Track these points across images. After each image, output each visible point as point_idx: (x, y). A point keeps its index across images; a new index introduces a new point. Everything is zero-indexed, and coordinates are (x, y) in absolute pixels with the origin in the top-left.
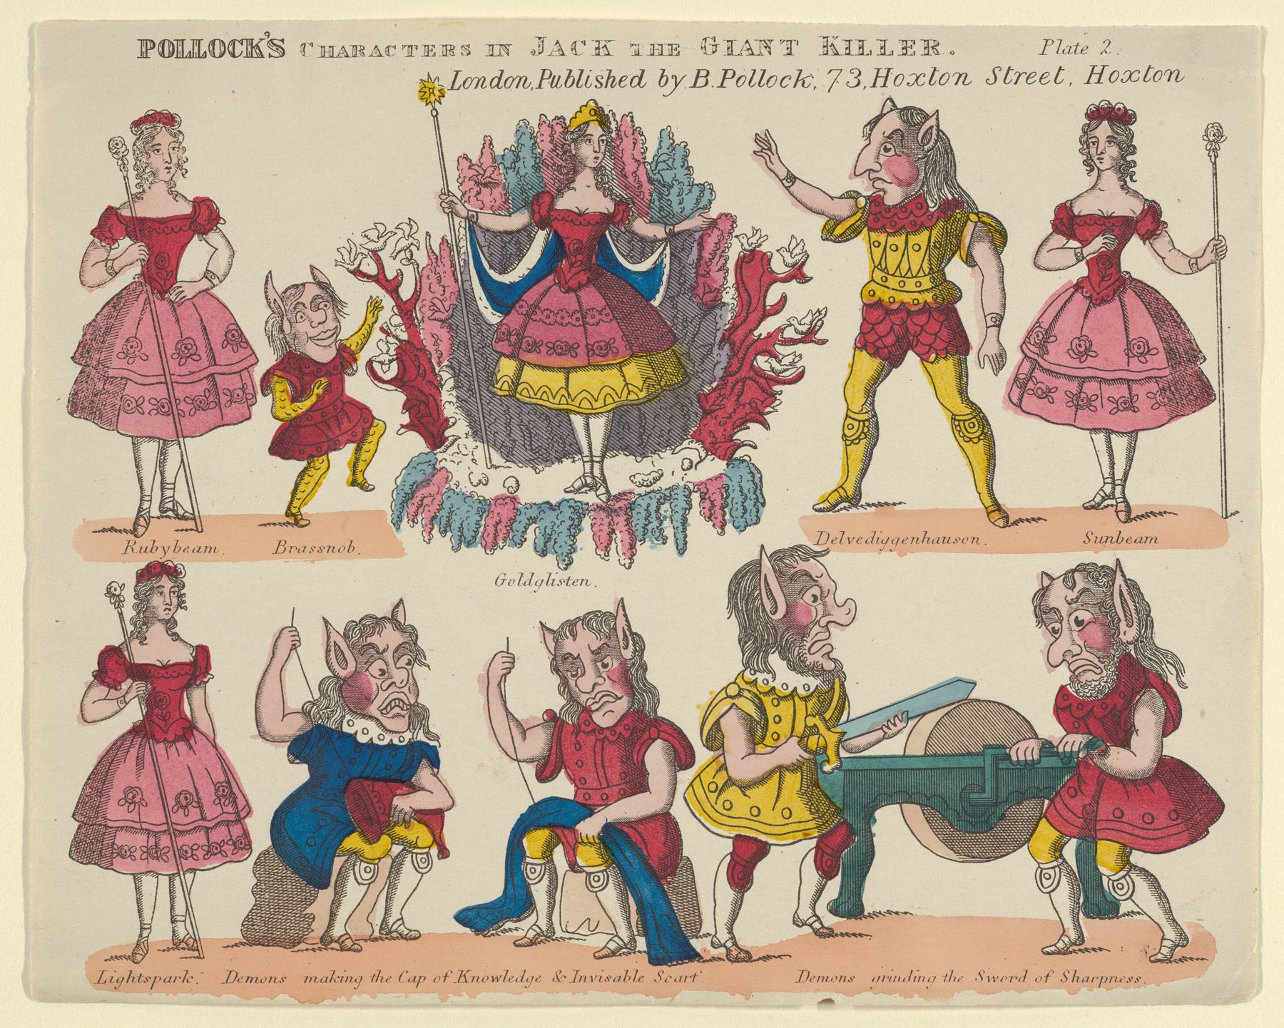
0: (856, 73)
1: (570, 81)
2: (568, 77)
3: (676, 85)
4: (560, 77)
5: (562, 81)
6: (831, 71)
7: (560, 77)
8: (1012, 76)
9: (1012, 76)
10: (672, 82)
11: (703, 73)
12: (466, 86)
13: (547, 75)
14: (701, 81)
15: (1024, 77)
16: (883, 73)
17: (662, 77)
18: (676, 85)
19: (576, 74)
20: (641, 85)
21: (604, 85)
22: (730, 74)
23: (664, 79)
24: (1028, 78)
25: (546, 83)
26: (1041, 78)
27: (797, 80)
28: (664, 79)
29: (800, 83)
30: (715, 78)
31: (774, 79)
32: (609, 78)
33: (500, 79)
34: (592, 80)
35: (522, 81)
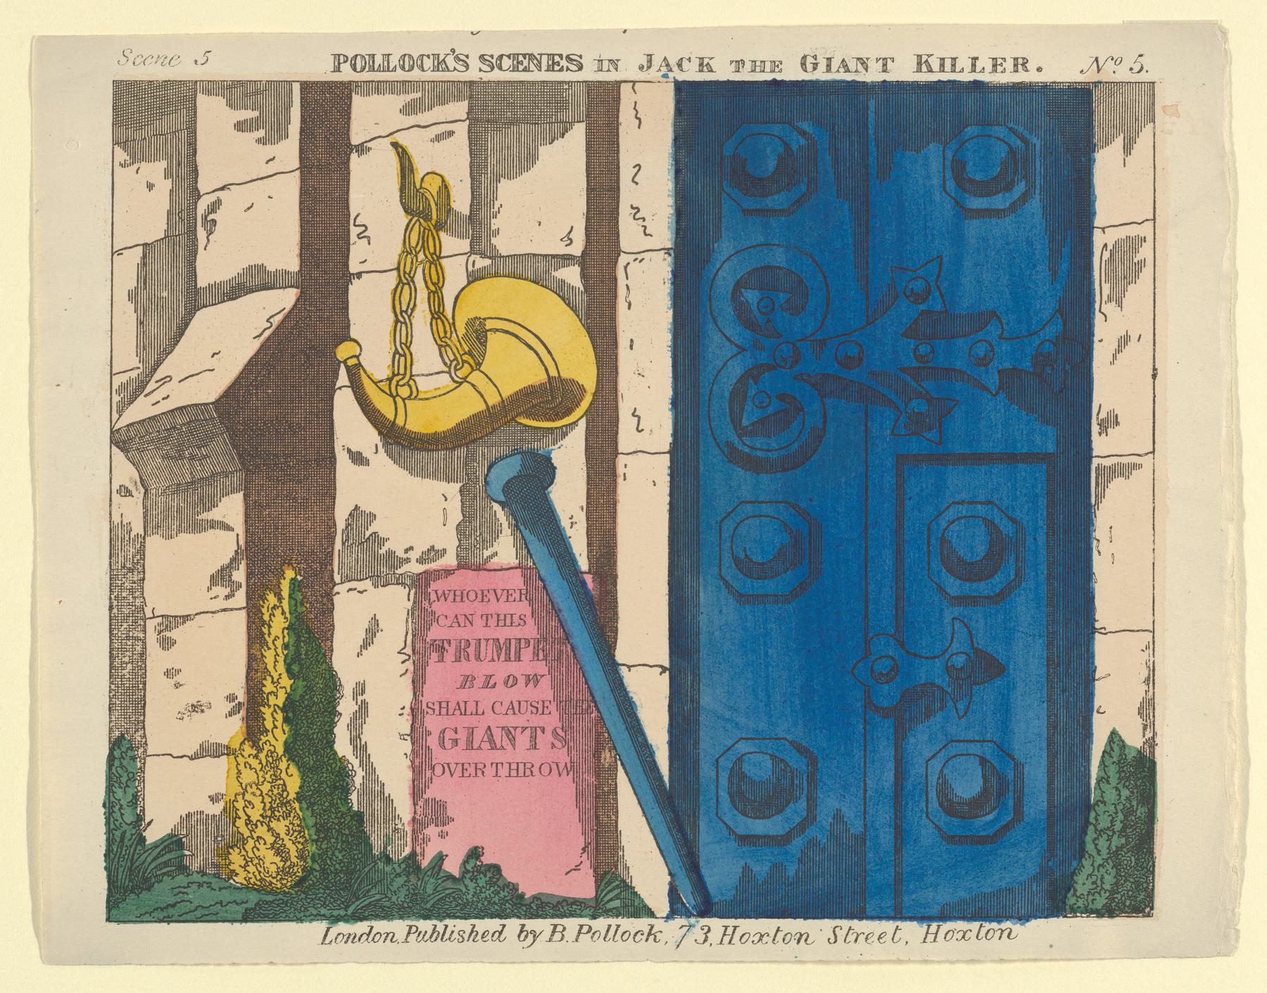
0: (706, 929)
1: (435, 935)
2: (433, 933)
3: (534, 941)
4: (426, 932)
5: (427, 937)
6: (683, 926)
7: (426, 932)
8: (851, 938)
9: (851, 938)
10: (531, 937)
11: (559, 928)
12: (338, 940)
13: (414, 929)
14: (557, 936)
15: (862, 938)
16: (730, 931)
17: (521, 932)
18: (534, 941)
19: (440, 928)
20: (501, 939)
21: (466, 936)
22: (585, 929)
23: (524, 934)
24: (867, 938)
25: (413, 937)
26: (880, 938)
27: (649, 934)
28: (525, 933)
29: (652, 938)
30: (571, 933)
31: (628, 933)
32: (472, 931)
33: (368, 935)
34: (455, 935)
35: (390, 937)
